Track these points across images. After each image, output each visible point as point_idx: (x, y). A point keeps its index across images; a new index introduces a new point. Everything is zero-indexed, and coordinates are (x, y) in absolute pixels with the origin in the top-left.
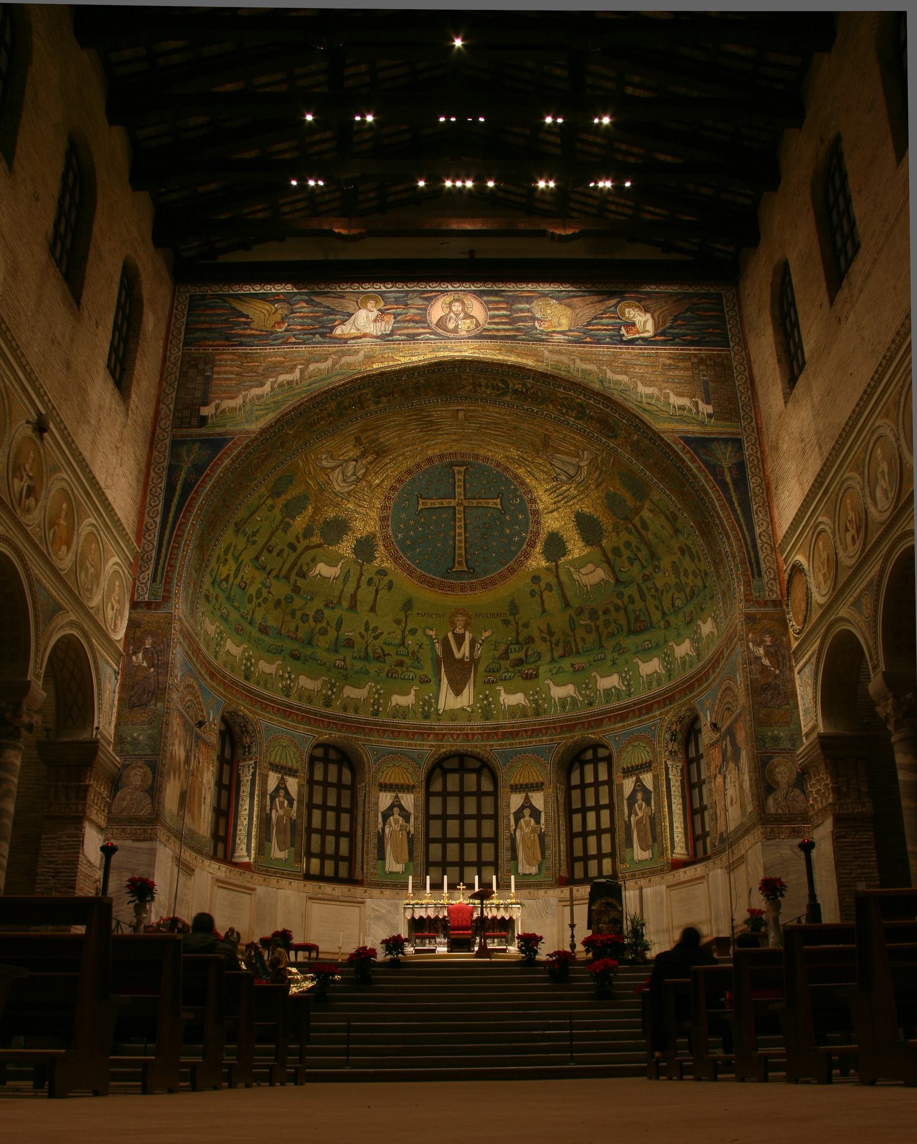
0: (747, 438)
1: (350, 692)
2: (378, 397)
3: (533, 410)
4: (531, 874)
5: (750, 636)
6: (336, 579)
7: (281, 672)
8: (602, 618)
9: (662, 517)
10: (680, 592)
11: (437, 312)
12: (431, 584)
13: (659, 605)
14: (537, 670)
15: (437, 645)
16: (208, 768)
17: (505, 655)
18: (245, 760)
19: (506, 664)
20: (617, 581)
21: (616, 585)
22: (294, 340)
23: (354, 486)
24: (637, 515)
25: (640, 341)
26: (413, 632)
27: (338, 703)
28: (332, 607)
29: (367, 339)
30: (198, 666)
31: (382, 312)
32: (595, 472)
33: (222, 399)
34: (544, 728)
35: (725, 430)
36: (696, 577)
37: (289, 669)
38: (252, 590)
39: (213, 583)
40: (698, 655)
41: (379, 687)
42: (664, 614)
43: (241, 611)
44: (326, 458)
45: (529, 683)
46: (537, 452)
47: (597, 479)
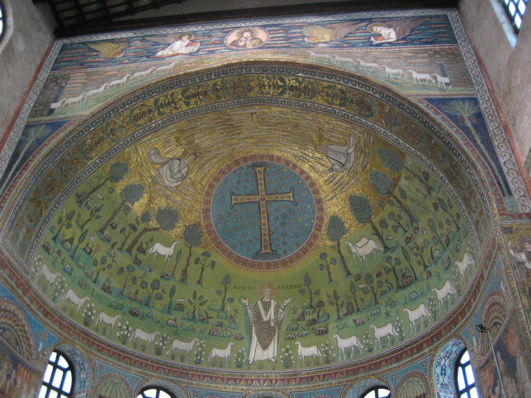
0: (481, 97)
1: (178, 345)
2: (188, 97)
3: (307, 105)
5: (509, 244)
6: (171, 257)
7: (120, 324)
8: (376, 280)
9: (416, 179)
10: (437, 244)
11: (232, 38)
12: (244, 263)
13: (420, 260)
14: (327, 327)
15: (249, 311)
16: (28, 392)
17: (302, 317)
18: (80, 393)
19: (303, 324)
20: (386, 248)
21: (385, 252)
22: (127, 61)
23: (180, 182)
24: (396, 186)
25: (386, 44)
26: (231, 300)
27: (167, 353)
28: (167, 279)
29: (179, 56)
30: (26, 299)
31: (192, 41)
32: (360, 156)
33: (68, 98)
34: (334, 373)
35: (461, 92)
36: (450, 224)
37: (127, 323)
38: (98, 256)
39: (54, 239)
40: (459, 291)
41: (202, 342)
42: (426, 266)
43: (86, 270)
44: (154, 154)
45: (322, 338)
46: (315, 146)
47: (363, 162)
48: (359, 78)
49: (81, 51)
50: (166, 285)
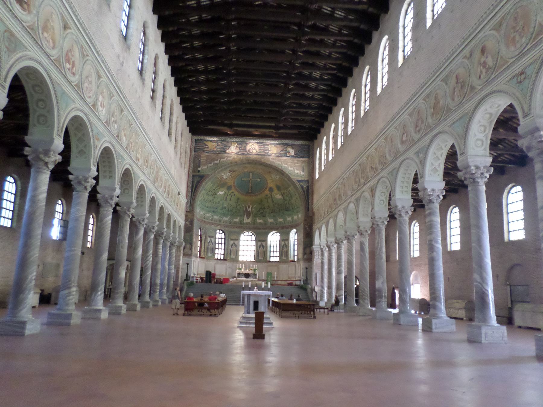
1: (225, 219)
4: (261, 260)
20: (284, 199)
26: (239, 205)
38: (206, 200)
48: (282, 170)
49: (202, 144)
50: (221, 202)
